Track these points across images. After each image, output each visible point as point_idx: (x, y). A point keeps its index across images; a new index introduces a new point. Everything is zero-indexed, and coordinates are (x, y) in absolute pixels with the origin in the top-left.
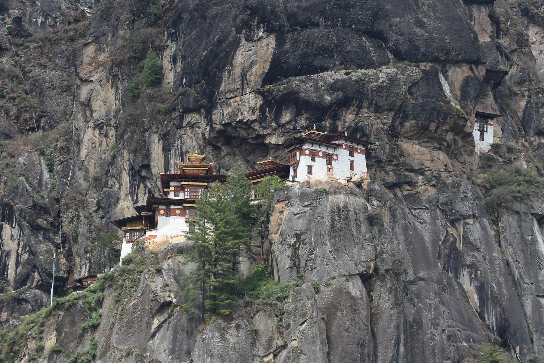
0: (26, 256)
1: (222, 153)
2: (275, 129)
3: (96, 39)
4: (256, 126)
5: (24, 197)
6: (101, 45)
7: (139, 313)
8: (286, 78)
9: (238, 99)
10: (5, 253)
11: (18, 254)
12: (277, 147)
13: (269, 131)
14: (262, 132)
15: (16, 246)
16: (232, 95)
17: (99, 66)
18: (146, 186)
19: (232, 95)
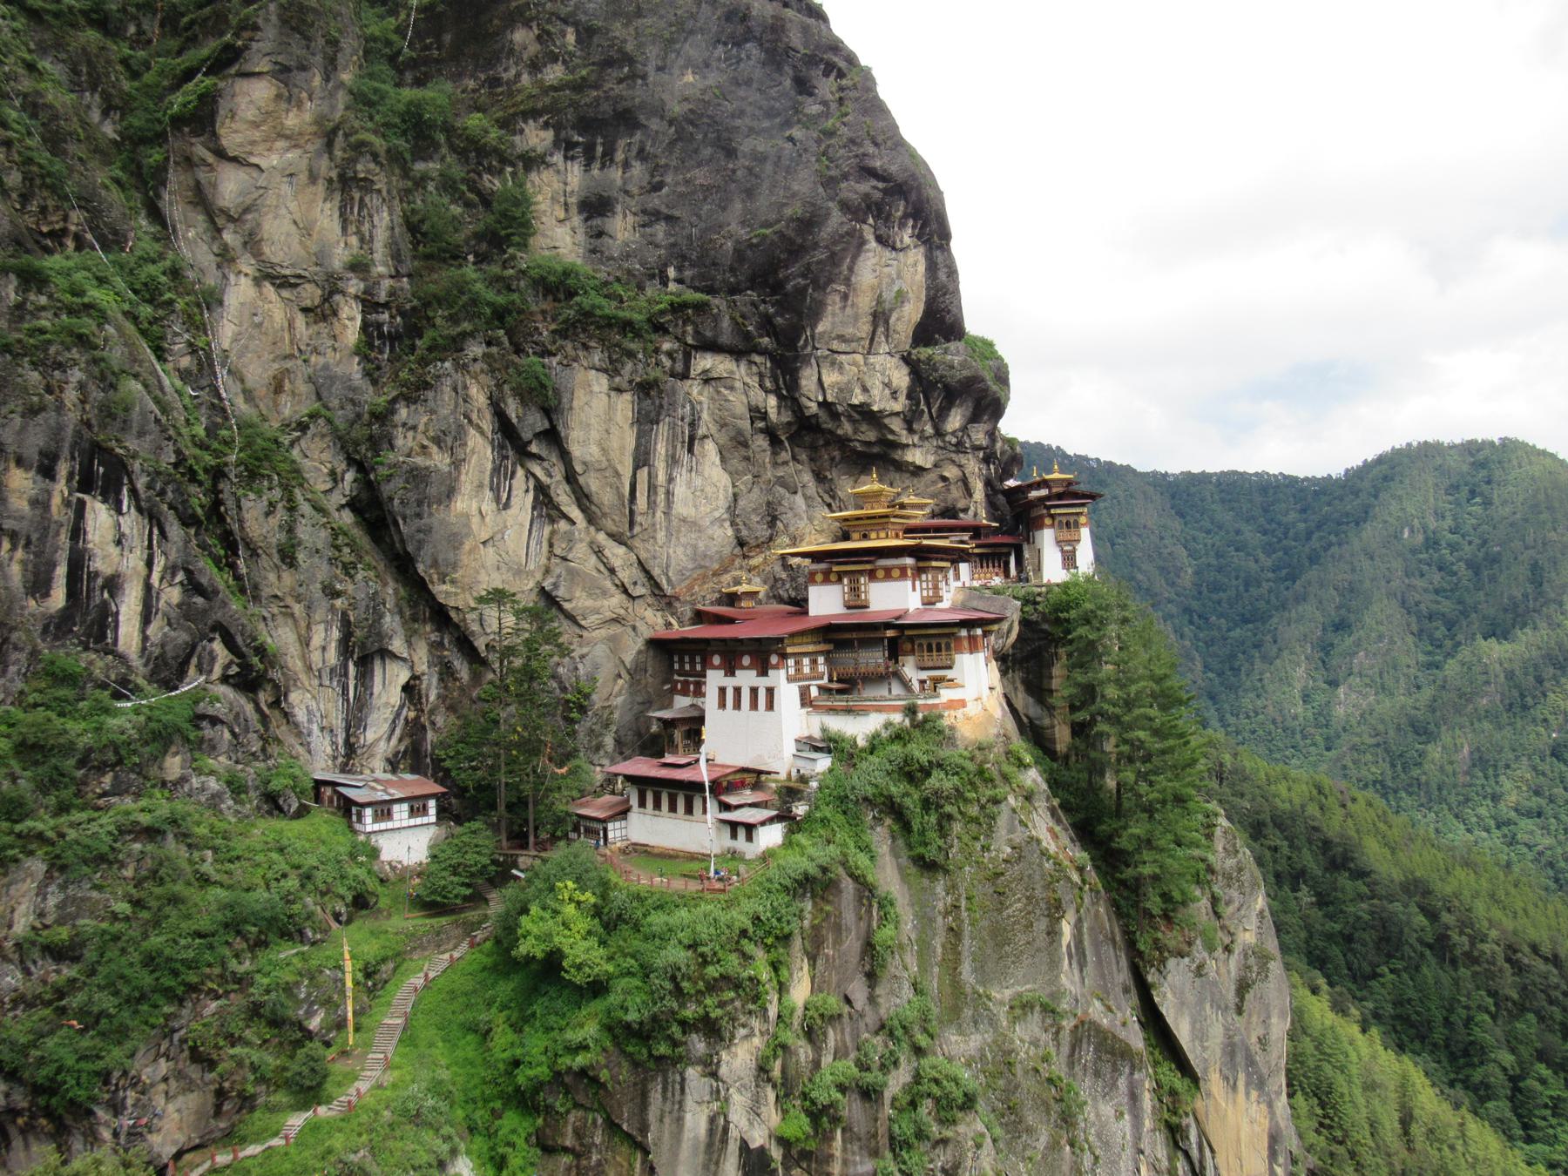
0: (173, 595)
1: (783, 454)
2: (923, 438)
3: (281, 72)
4: (896, 425)
5: (148, 438)
6: (296, 90)
7: (1019, 905)
8: (948, 341)
9: (859, 358)
10: (100, 581)
11: (148, 587)
12: (918, 471)
13: (916, 439)
14: (905, 438)
15: (133, 562)
16: (843, 347)
17: (281, 136)
18: (529, 474)
19: (843, 347)
